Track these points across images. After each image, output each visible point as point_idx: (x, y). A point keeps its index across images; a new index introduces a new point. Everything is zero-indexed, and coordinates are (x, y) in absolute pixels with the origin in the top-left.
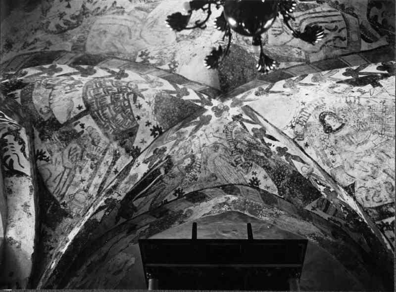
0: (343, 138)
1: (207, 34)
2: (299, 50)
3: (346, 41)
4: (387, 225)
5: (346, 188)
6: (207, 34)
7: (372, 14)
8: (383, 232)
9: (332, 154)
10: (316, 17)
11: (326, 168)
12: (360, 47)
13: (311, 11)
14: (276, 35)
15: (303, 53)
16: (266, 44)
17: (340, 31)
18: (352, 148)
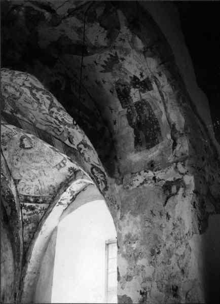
0: (27, 154)
3: (60, 133)
4: (25, 206)
5: (14, 180)
8: (21, 209)
9: (17, 160)
11: (10, 166)
18: (29, 162)
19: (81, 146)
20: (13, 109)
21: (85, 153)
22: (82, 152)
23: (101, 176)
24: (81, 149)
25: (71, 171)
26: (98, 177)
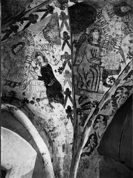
0: (9, 55)
1: (110, 12)
2: (80, 61)
3: (80, 88)
6: (110, 12)
7: (101, 116)
10: (97, 80)
12: (77, 95)
13: (101, 79)
14: (92, 50)
15: (79, 63)
16: (88, 42)
17: (86, 86)
19: (102, 118)
20: (77, 42)
21: (99, 123)
22: (98, 120)
23: (93, 144)
24: (100, 118)
25: (12, 94)
26: (91, 143)
